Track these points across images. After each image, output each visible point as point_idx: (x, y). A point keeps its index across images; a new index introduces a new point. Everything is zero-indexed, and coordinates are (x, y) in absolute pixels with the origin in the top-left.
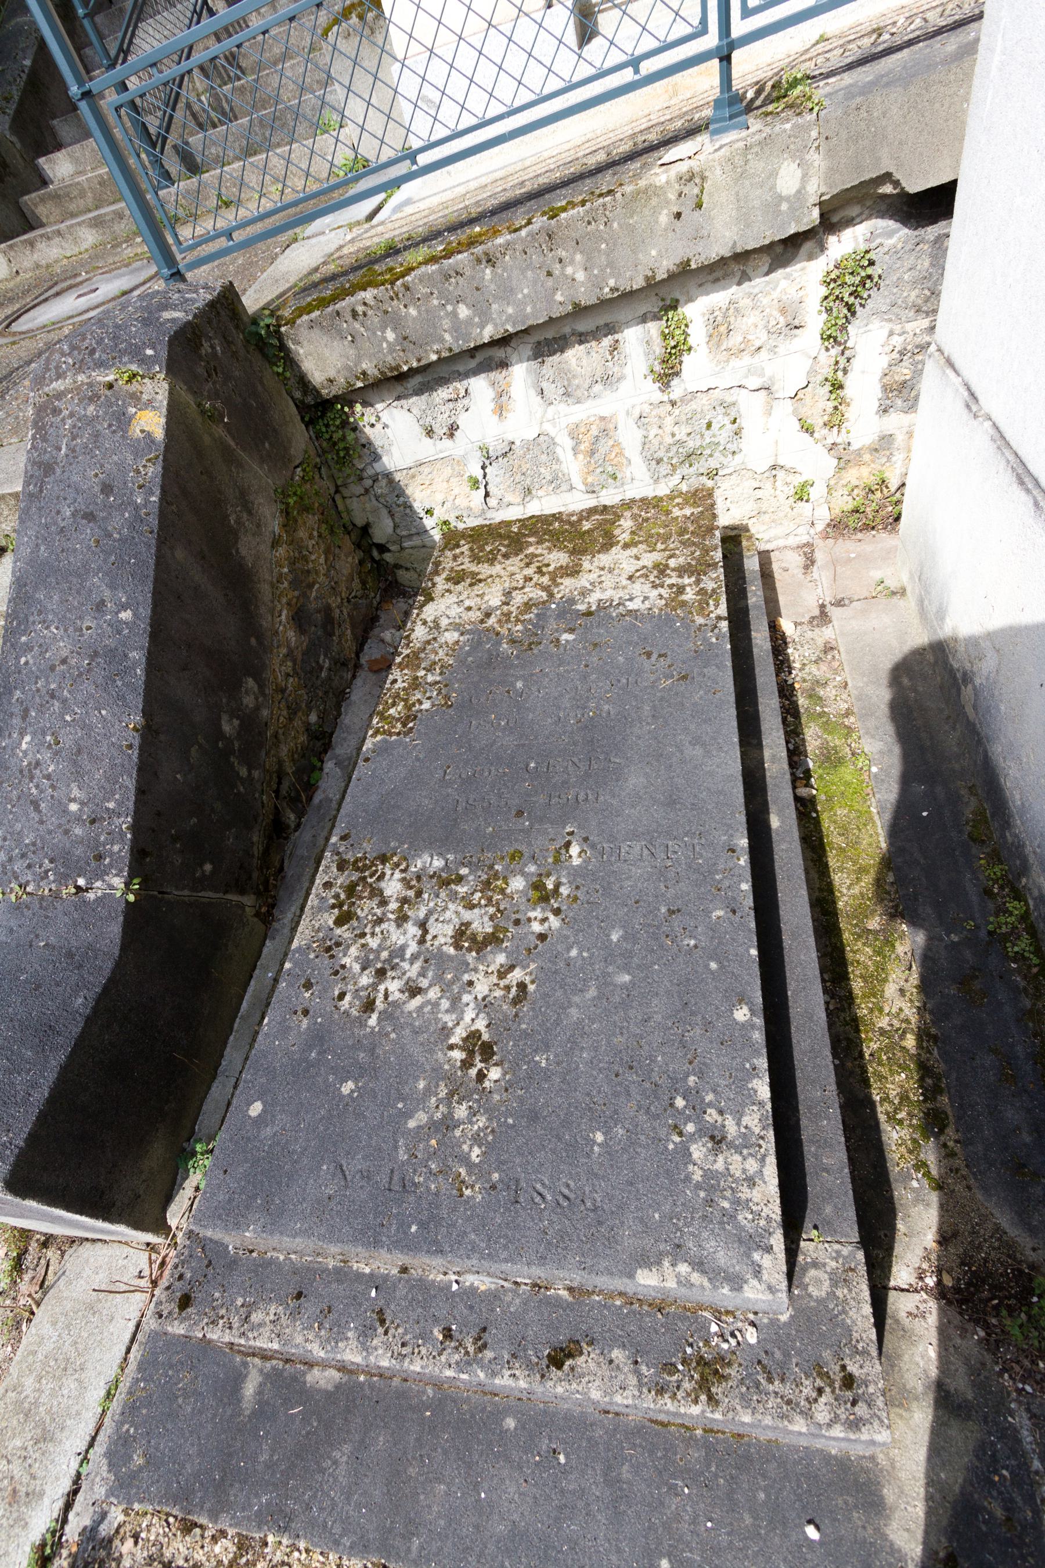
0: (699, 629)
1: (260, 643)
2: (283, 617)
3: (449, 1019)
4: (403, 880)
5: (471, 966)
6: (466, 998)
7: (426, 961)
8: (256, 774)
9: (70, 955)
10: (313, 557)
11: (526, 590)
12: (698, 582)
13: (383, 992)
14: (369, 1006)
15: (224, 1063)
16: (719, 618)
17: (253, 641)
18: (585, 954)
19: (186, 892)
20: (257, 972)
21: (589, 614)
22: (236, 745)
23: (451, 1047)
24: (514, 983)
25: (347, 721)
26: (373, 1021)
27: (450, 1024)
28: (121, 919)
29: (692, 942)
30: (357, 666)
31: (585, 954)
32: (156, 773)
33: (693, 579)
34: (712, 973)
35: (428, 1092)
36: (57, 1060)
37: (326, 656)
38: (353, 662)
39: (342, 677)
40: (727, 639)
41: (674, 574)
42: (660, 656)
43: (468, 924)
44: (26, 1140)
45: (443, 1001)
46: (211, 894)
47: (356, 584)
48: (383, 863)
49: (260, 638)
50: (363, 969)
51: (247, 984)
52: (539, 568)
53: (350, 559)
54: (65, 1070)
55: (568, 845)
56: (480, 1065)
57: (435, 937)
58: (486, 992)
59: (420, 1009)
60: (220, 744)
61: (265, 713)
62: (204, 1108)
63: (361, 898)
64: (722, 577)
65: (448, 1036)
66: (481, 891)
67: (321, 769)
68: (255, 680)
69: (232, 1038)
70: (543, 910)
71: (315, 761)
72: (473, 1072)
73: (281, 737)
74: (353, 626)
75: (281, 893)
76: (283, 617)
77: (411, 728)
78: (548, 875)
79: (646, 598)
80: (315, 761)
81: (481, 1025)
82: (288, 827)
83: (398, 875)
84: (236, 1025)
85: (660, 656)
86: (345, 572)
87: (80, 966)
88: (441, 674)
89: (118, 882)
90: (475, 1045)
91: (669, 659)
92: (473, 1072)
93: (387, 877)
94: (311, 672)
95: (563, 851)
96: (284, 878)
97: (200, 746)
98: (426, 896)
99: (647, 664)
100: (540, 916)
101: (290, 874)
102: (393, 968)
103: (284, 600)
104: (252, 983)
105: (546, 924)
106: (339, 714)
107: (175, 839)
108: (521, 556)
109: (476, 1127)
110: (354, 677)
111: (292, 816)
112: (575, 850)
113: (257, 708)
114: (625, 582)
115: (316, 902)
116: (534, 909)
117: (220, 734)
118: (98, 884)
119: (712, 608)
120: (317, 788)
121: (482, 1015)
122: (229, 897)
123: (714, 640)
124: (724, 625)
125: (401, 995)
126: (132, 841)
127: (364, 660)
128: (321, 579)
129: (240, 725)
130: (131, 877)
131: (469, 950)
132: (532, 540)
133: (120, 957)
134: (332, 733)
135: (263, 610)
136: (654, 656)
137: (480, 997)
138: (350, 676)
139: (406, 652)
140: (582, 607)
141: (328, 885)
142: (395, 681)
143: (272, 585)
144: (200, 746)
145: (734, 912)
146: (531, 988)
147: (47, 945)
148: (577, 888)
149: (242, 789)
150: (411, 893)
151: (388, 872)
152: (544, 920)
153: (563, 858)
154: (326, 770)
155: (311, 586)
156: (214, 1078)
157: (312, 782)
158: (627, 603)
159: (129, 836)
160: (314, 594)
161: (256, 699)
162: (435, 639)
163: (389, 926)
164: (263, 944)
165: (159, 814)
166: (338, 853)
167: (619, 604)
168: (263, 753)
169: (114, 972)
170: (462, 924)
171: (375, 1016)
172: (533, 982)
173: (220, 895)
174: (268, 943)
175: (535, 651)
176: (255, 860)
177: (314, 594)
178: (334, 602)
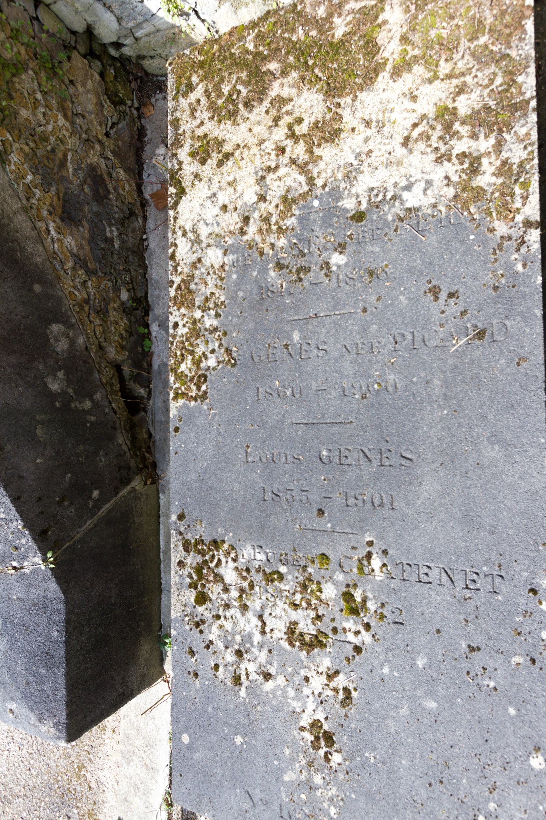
0: (500, 247)
1: (43, 282)
2: (53, 232)
3: (297, 705)
4: (236, 569)
5: (305, 664)
6: (306, 691)
7: (270, 651)
8: (98, 396)
9: (35, 605)
10: (50, 128)
11: (282, 171)
12: (499, 146)
13: (244, 669)
14: (237, 680)
15: (163, 582)
16: (528, 224)
17: (37, 288)
18: (396, 674)
19: (89, 522)
20: (161, 519)
21: (359, 217)
22: (71, 391)
23: (302, 729)
24: (341, 687)
25: (154, 276)
26: (243, 693)
27: (298, 710)
28: (53, 579)
29: (492, 684)
30: (144, 204)
31: (396, 674)
32: (20, 477)
33: (492, 141)
34: (511, 718)
35: (293, 760)
36: (61, 672)
37: (110, 225)
38: (138, 204)
39: (134, 231)
40: (538, 265)
41: (464, 130)
42: (451, 295)
43: (296, 623)
44: (67, 719)
45: (289, 689)
46: (107, 506)
47: (108, 109)
48: (217, 549)
49: (41, 278)
50: (227, 648)
51: (158, 528)
52: (290, 127)
53: (90, 85)
54: (68, 676)
55: (369, 556)
56: (325, 749)
57: (272, 630)
58: (320, 690)
59: (274, 691)
60: (57, 404)
61: (81, 341)
62: (162, 611)
63: (208, 581)
64: (534, 136)
65: (298, 719)
66: (301, 593)
67: (150, 333)
68: (58, 322)
69: (162, 566)
70: (355, 623)
71: (142, 330)
72: (322, 752)
73: (104, 344)
74: (123, 161)
75: (157, 456)
76: (53, 232)
77: (205, 393)
78: (355, 586)
79: (429, 183)
80: (142, 330)
81: (320, 716)
82: (142, 398)
83: (231, 564)
84: (162, 558)
85: (451, 295)
86: (91, 107)
87: (45, 612)
88: (217, 315)
89: (38, 560)
90: (319, 733)
91: (461, 302)
92: (322, 752)
93: (223, 564)
94: (104, 256)
95: (365, 563)
96: (154, 442)
97: (42, 423)
98: (257, 589)
99: (435, 308)
100: (353, 629)
101: (157, 438)
102: (247, 652)
103: (45, 213)
104: (161, 527)
105: (359, 637)
106: (146, 268)
107: (63, 500)
108: (266, 104)
109: (330, 794)
110: (145, 218)
111: (142, 391)
112: (376, 563)
113: (72, 343)
114: (401, 151)
115: (177, 578)
116: (347, 620)
117: (51, 396)
118: (26, 563)
119: (518, 204)
120: (152, 354)
121: (320, 708)
122: (121, 494)
123: (519, 267)
124: (535, 235)
125: (257, 677)
126: (30, 534)
127: (147, 196)
128: (71, 142)
129: (66, 374)
130: (44, 554)
131: (301, 649)
132: (273, 66)
133: (66, 598)
134: (147, 293)
135: (30, 246)
136: (443, 296)
137: (316, 693)
138: (140, 220)
139: (177, 280)
140: (349, 204)
141: (181, 564)
142: (176, 325)
143: (26, 210)
144: (42, 423)
145: (533, 661)
146: (354, 694)
147: (18, 598)
148: (383, 605)
149: (93, 418)
150: (245, 585)
151: (223, 560)
152: (357, 633)
153: (366, 570)
154: (154, 334)
155: (63, 164)
156: (161, 591)
157: (146, 350)
158: (405, 195)
159: (27, 532)
160: (71, 169)
161: (68, 336)
162: (199, 260)
163: (234, 612)
164: (158, 498)
165: (39, 499)
166: (181, 533)
167: (394, 198)
168: (96, 375)
169: (67, 609)
170: (291, 623)
171: (243, 689)
172: (355, 689)
173: (114, 499)
174: (161, 496)
175: (306, 284)
176: (128, 454)
177: (71, 169)
178: (93, 158)
